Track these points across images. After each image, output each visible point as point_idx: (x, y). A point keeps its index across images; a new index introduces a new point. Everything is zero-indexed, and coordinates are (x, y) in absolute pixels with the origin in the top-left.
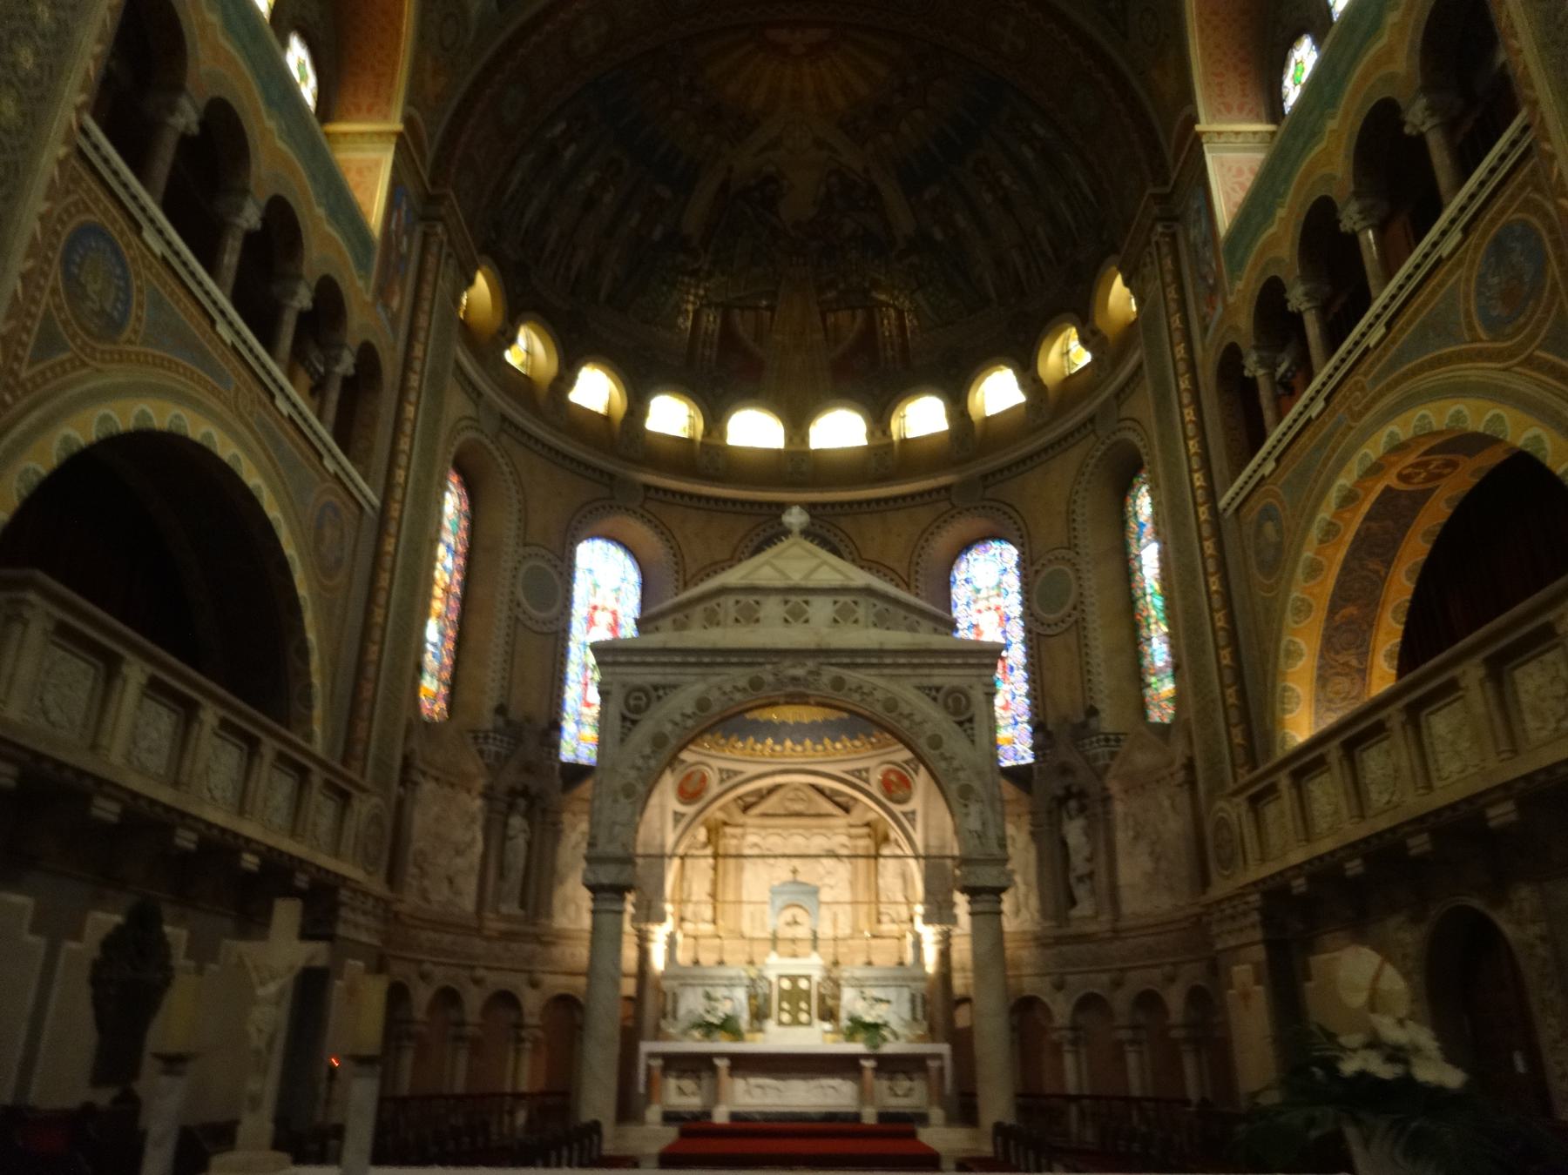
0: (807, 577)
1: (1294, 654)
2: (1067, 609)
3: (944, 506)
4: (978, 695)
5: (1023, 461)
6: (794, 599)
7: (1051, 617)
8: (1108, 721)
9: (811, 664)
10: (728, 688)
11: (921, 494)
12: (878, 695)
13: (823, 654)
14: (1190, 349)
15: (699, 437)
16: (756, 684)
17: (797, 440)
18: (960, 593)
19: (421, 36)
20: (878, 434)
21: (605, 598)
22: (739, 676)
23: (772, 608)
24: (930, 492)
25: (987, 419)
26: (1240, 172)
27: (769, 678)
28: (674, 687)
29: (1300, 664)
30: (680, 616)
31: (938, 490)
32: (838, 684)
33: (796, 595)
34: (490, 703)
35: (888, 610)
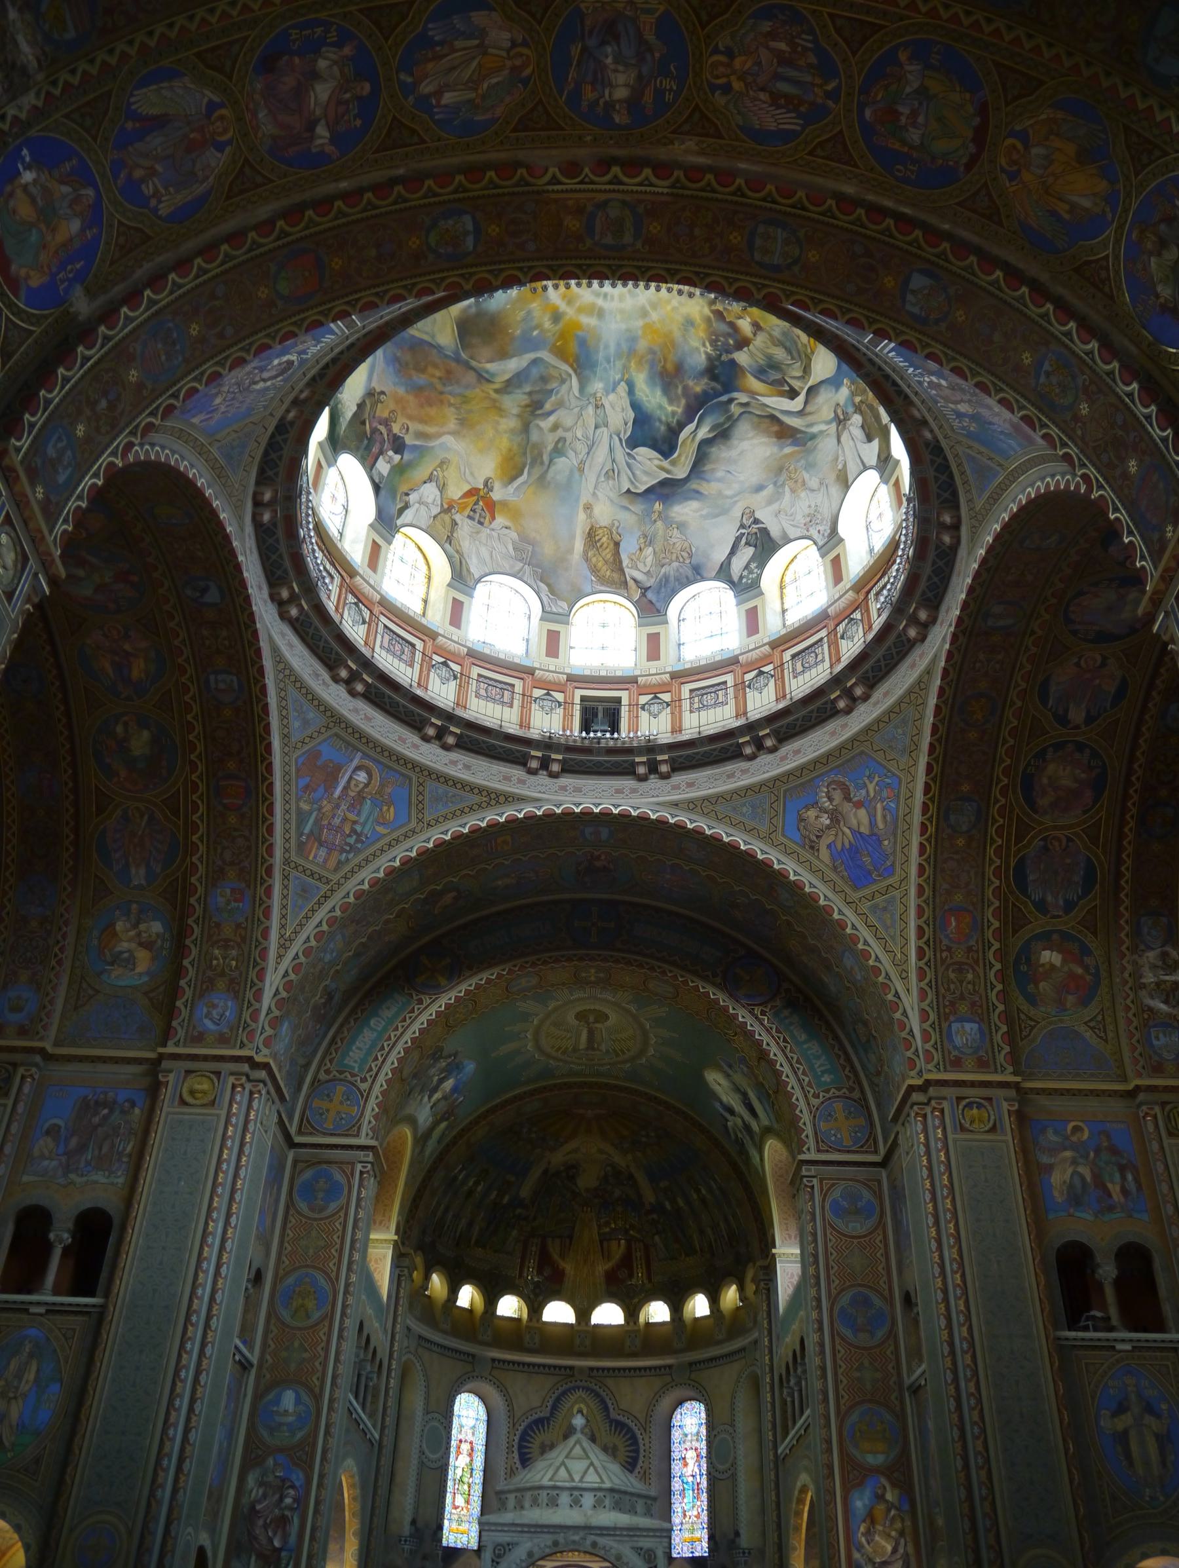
0: (581, 1481)
1: (795, 1549)
2: (727, 1465)
3: (668, 1379)
4: (660, 1553)
5: (711, 1359)
6: (576, 1493)
7: (721, 1467)
8: (744, 1541)
9: (582, 1533)
10: (542, 1545)
11: (655, 1368)
12: (613, 1551)
13: (588, 1528)
14: (771, 1359)
15: (525, 1316)
16: (556, 1543)
17: (583, 1324)
18: (676, 1435)
19: (406, 1184)
20: (632, 1324)
21: (467, 1434)
22: (547, 1539)
23: (564, 1498)
24: (660, 1368)
25: (697, 1320)
26: (792, 1275)
27: (561, 1541)
28: (517, 1544)
29: (797, 1553)
30: (518, 1495)
31: (665, 1367)
32: (594, 1544)
33: (576, 1493)
34: (408, 1519)
35: (620, 1499)
